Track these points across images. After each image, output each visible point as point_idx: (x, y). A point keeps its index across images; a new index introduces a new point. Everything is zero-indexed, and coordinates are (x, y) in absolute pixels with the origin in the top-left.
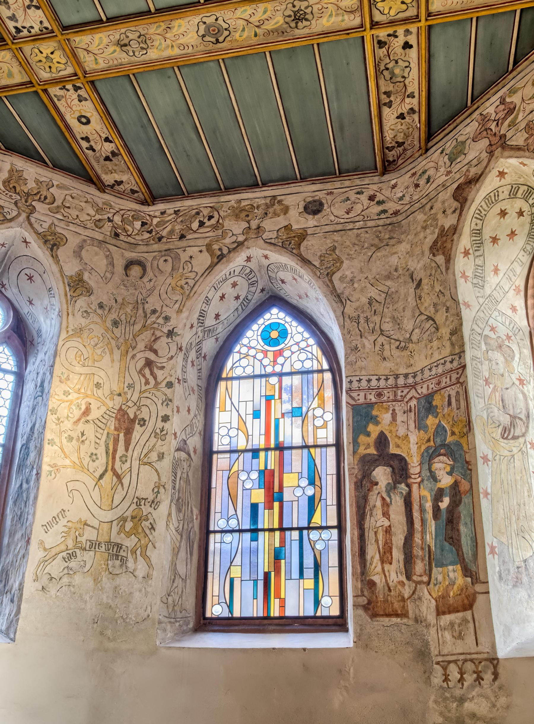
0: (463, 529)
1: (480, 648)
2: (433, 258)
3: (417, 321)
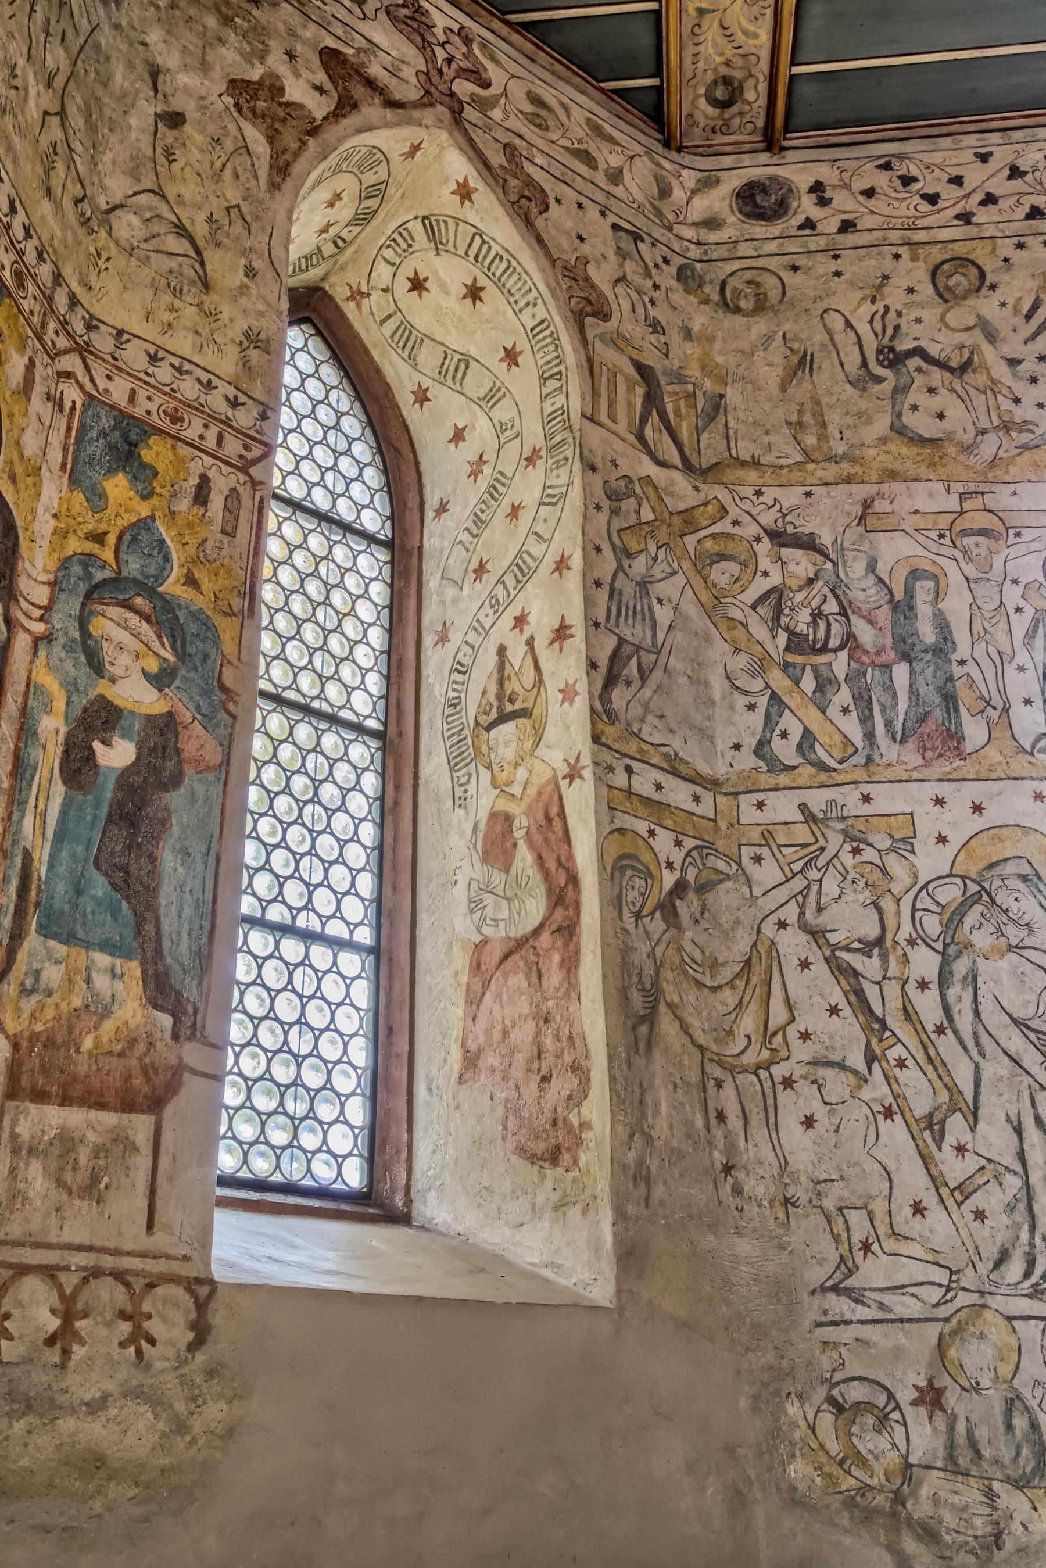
0: (169, 860)
1: (159, 1240)
2: (236, 114)
3: (143, 199)
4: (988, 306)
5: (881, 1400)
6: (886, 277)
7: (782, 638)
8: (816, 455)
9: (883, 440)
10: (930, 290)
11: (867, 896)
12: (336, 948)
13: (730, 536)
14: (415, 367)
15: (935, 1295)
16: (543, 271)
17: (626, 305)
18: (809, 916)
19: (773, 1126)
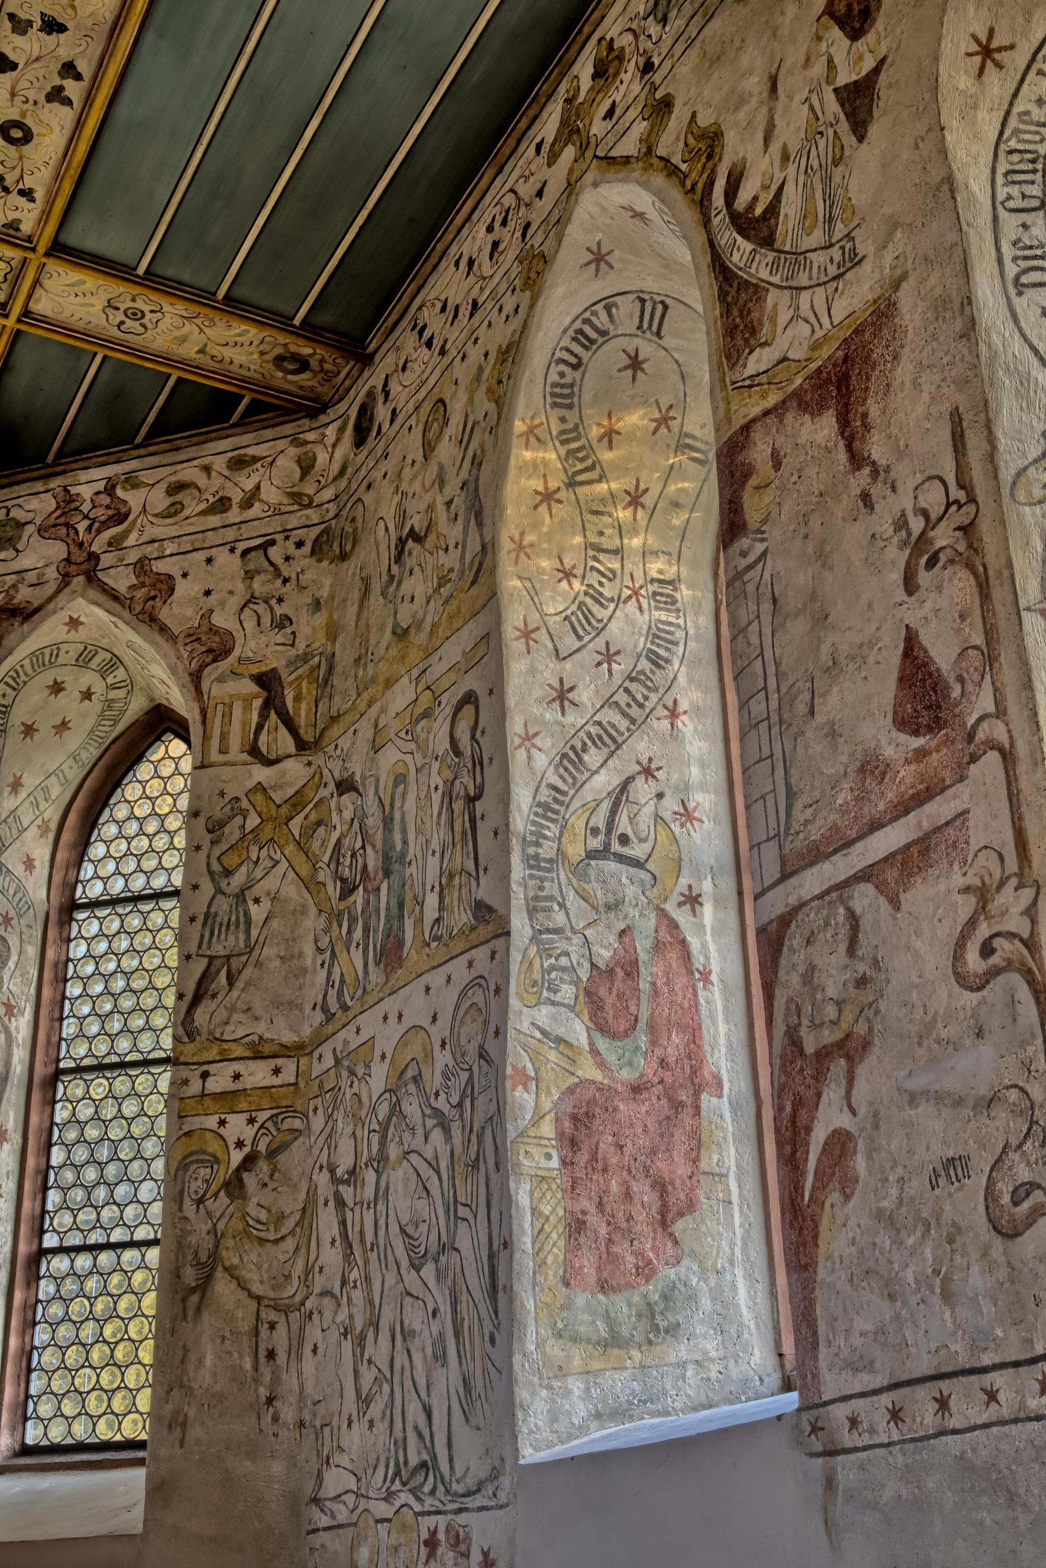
17: (250, 624)
19: (300, 1357)
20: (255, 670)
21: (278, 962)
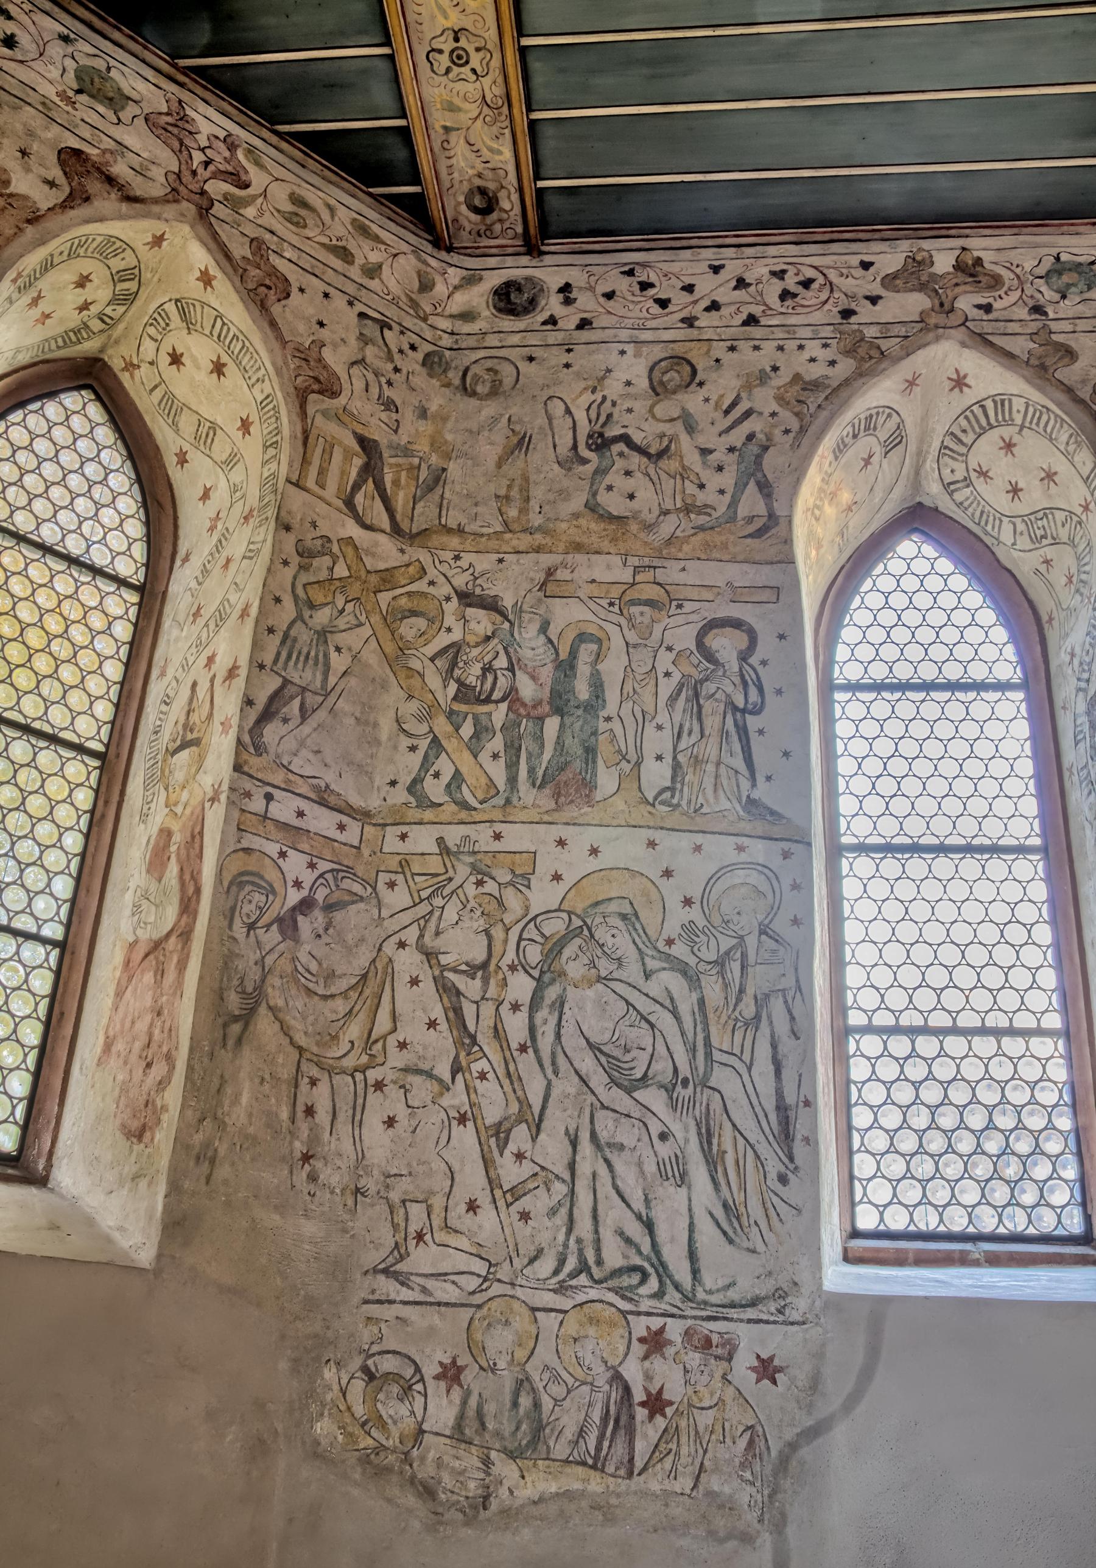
4: (693, 401)
5: (408, 1372)
6: (609, 371)
7: (453, 687)
8: (515, 526)
9: (576, 516)
10: (645, 383)
11: (481, 924)
12: (20, 940)
13: (423, 595)
14: (177, 431)
15: (473, 1283)
16: (271, 351)
17: (358, 385)
18: (427, 939)
20: (360, 430)
21: (352, 721)
